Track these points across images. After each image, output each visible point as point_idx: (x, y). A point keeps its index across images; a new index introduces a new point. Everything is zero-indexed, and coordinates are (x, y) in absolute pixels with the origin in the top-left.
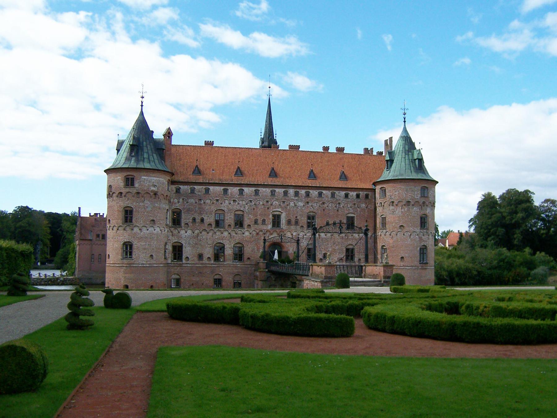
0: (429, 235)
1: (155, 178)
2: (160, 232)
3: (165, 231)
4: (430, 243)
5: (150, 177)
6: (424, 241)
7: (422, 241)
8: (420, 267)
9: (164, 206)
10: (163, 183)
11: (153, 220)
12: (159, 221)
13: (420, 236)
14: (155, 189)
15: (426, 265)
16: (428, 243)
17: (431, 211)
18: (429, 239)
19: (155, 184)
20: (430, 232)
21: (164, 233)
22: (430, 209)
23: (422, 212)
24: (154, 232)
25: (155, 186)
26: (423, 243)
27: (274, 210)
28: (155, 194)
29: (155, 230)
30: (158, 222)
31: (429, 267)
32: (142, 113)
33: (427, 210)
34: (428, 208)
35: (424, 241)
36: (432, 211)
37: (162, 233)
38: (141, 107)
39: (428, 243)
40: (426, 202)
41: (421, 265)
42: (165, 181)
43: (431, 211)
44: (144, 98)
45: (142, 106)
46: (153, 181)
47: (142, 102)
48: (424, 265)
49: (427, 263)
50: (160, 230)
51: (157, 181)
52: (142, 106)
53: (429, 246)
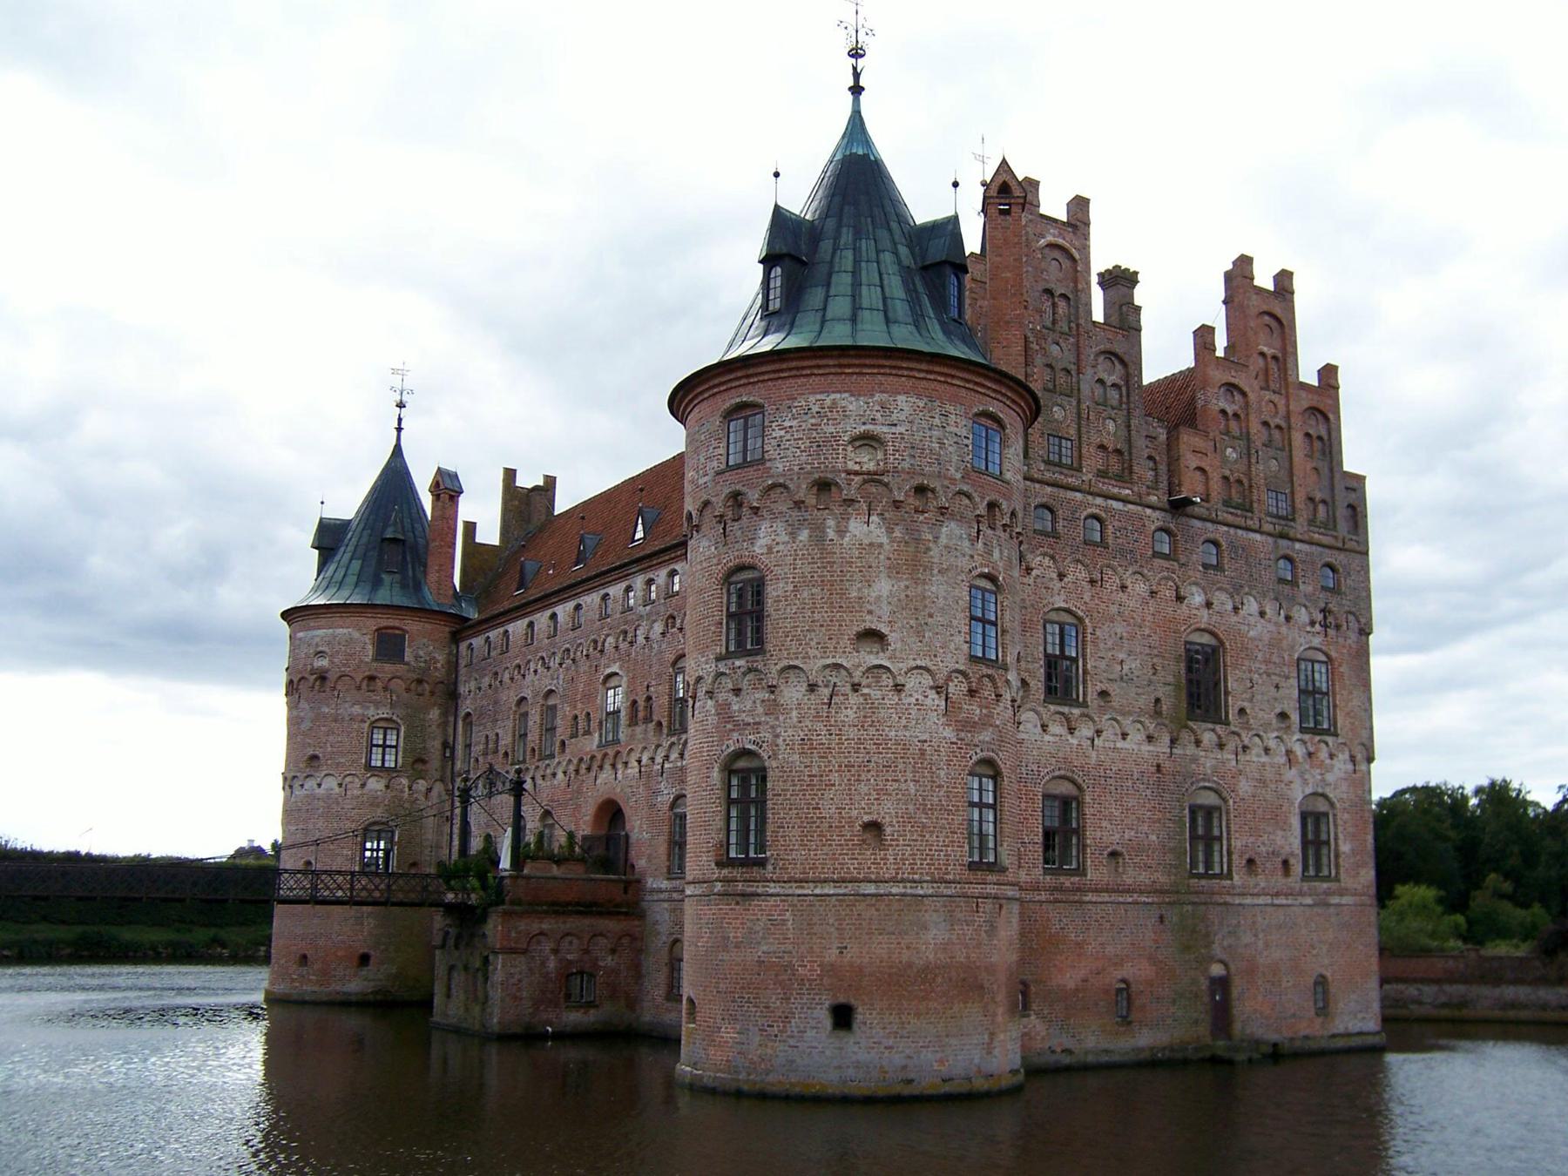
0: (772, 689)
1: (321, 632)
2: (337, 790)
3: (363, 785)
4: (786, 734)
5: (309, 632)
6: (741, 726)
7: (729, 726)
8: (719, 887)
9: (357, 710)
10: (350, 641)
11: (314, 758)
12: (331, 759)
13: (722, 697)
14: (323, 663)
15: (756, 872)
16: (769, 736)
17: (793, 535)
18: (773, 708)
19: (320, 649)
20: (774, 670)
21: (357, 792)
22: (780, 526)
23: (731, 559)
24: (318, 791)
25: (320, 654)
26: (735, 735)
27: (608, 671)
28: (322, 678)
29: (319, 785)
30: (329, 762)
31: (773, 889)
32: (397, 451)
33: (752, 541)
34: (764, 527)
35: (741, 726)
36: (804, 535)
37: (348, 793)
38: (395, 433)
39: (769, 736)
40: (744, 489)
41: (725, 872)
42: (356, 635)
43: (793, 535)
44: (404, 407)
45: (399, 429)
46: (318, 639)
47: (400, 420)
48: (736, 873)
49: (762, 863)
50: (340, 785)
51: (327, 639)
52: (399, 429)
53: (774, 756)
